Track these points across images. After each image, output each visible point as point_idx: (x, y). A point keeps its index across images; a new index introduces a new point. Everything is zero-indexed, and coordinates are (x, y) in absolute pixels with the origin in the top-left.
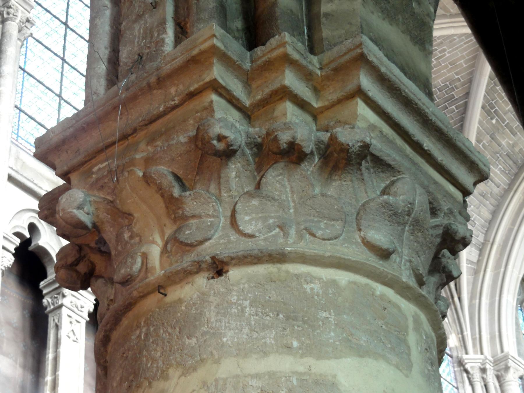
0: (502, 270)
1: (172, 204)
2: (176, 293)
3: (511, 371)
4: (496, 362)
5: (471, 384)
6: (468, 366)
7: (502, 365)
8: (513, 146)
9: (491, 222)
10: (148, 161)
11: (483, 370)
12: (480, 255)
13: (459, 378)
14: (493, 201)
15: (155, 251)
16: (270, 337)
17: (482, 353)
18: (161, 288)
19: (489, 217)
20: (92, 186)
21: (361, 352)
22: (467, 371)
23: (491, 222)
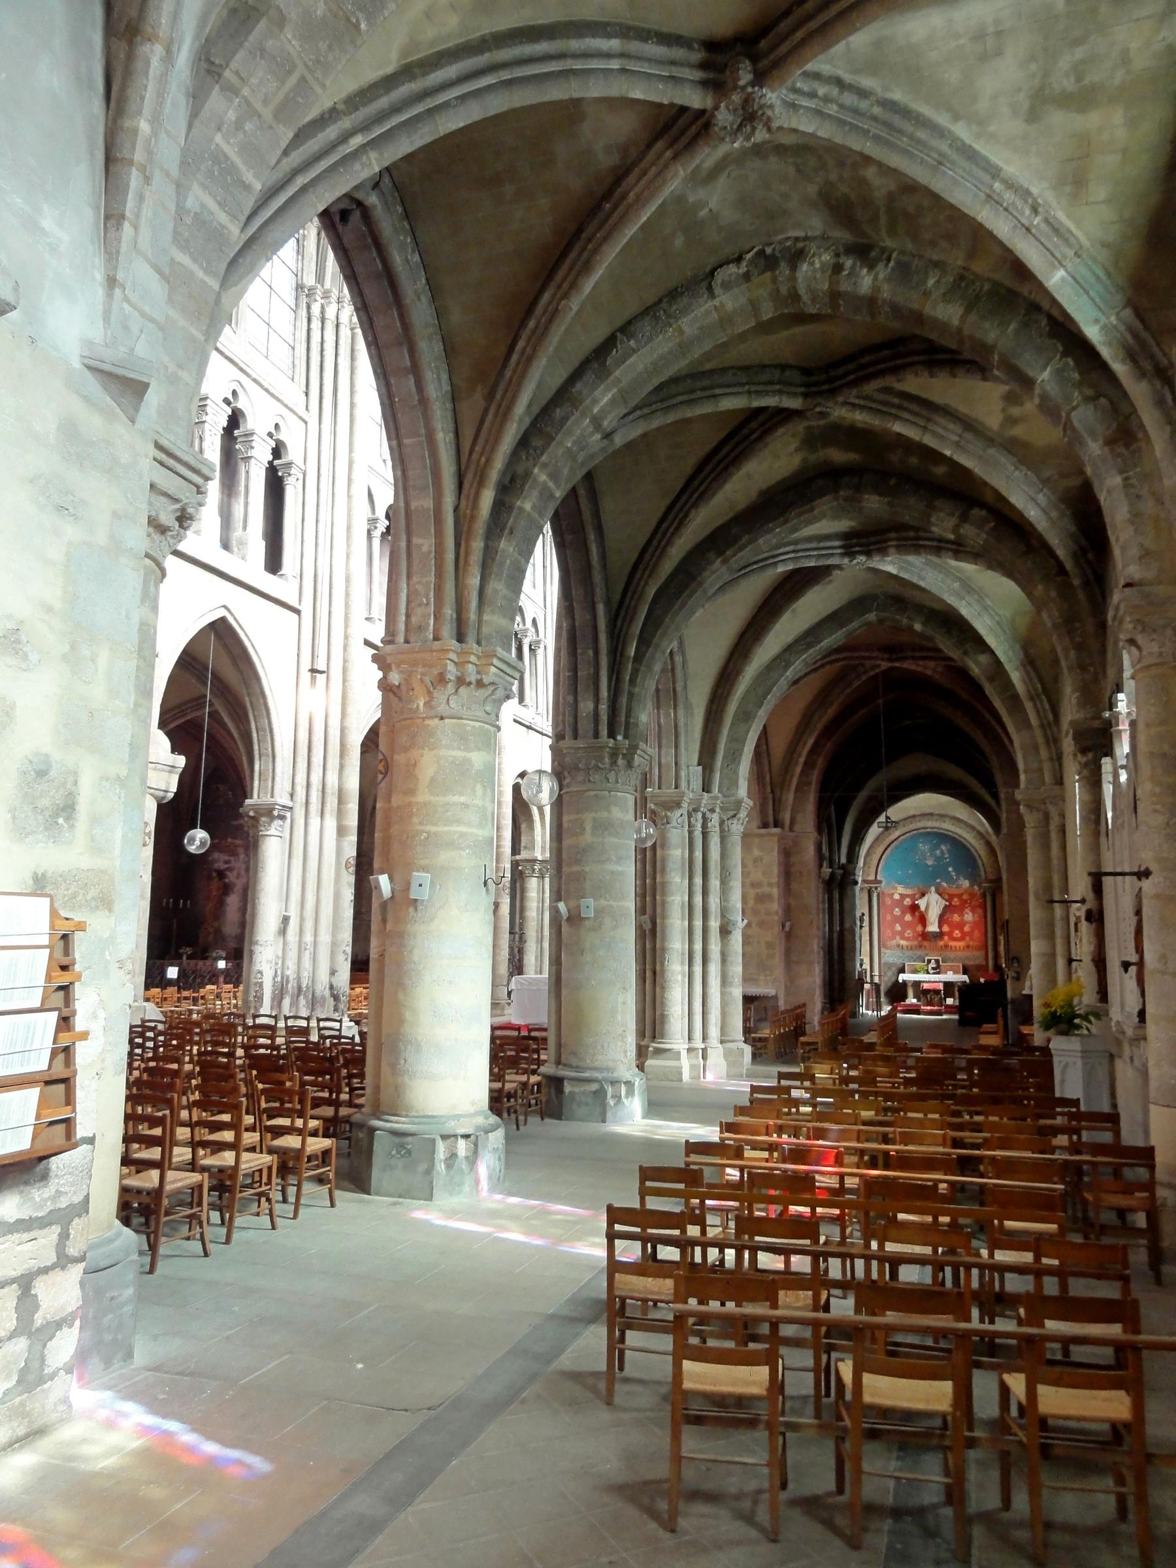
1: (429, 692)
2: (427, 722)
10: (423, 674)
15: (422, 704)
16: (455, 744)
18: (424, 719)
20: (401, 672)
21: (479, 750)
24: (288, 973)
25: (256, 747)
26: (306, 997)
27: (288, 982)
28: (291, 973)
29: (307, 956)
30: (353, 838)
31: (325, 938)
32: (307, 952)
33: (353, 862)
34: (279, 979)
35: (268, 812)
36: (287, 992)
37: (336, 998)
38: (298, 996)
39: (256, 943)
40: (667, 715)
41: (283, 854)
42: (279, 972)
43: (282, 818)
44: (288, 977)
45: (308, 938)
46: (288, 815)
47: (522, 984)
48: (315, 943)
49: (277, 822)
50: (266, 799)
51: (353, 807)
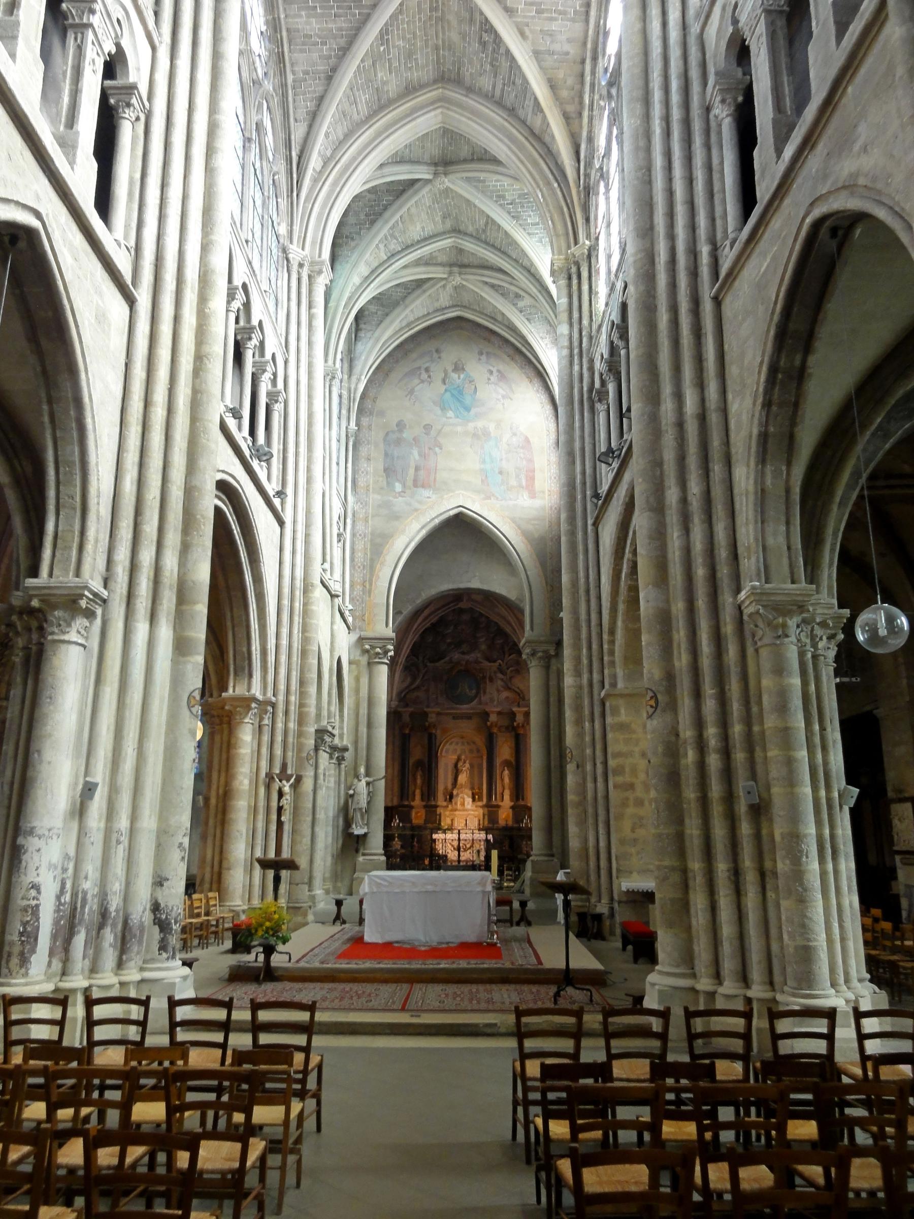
0: (338, 189)
3: (323, 276)
4: (312, 263)
5: (288, 271)
6: (291, 256)
7: (317, 268)
8: (384, 83)
9: (341, 143)
11: (301, 265)
12: (323, 167)
13: (280, 262)
14: (349, 125)
17: (303, 249)
19: (342, 137)
22: (288, 260)
23: (341, 143)
24: (87, 885)
25: (51, 493)
26: (114, 925)
27: (84, 901)
28: (89, 886)
29: (119, 855)
30: (198, 659)
31: (149, 822)
32: (121, 848)
33: (197, 695)
34: (67, 897)
35: (72, 603)
36: (82, 920)
37: (163, 926)
38: (101, 926)
39: (31, 832)
40: (776, 474)
41: (86, 675)
42: (68, 886)
43: (89, 614)
44: (85, 893)
45: (123, 823)
46: (99, 612)
47: (378, 885)
48: (132, 831)
49: (80, 622)
50: (65, 579)
51: (201, 609)
